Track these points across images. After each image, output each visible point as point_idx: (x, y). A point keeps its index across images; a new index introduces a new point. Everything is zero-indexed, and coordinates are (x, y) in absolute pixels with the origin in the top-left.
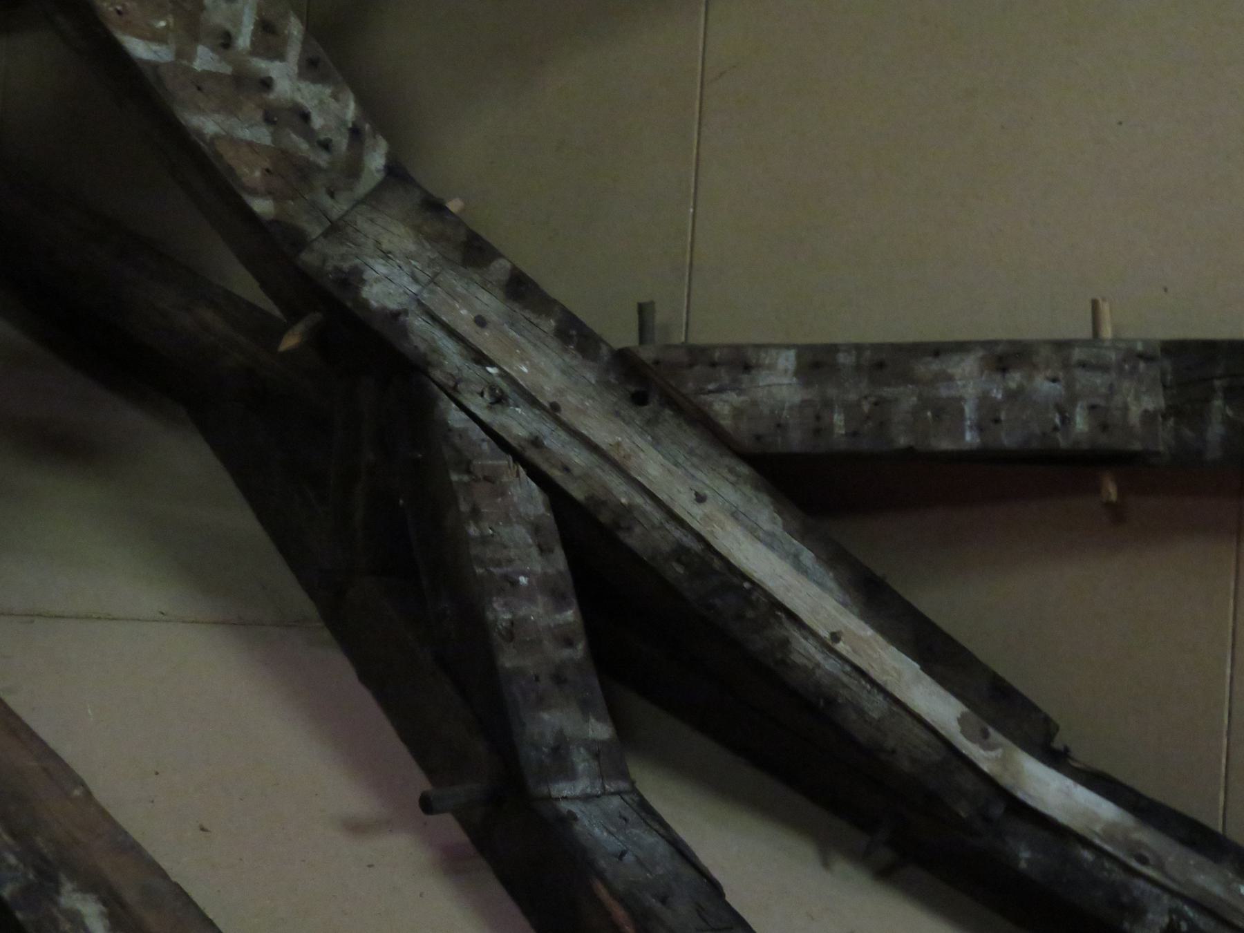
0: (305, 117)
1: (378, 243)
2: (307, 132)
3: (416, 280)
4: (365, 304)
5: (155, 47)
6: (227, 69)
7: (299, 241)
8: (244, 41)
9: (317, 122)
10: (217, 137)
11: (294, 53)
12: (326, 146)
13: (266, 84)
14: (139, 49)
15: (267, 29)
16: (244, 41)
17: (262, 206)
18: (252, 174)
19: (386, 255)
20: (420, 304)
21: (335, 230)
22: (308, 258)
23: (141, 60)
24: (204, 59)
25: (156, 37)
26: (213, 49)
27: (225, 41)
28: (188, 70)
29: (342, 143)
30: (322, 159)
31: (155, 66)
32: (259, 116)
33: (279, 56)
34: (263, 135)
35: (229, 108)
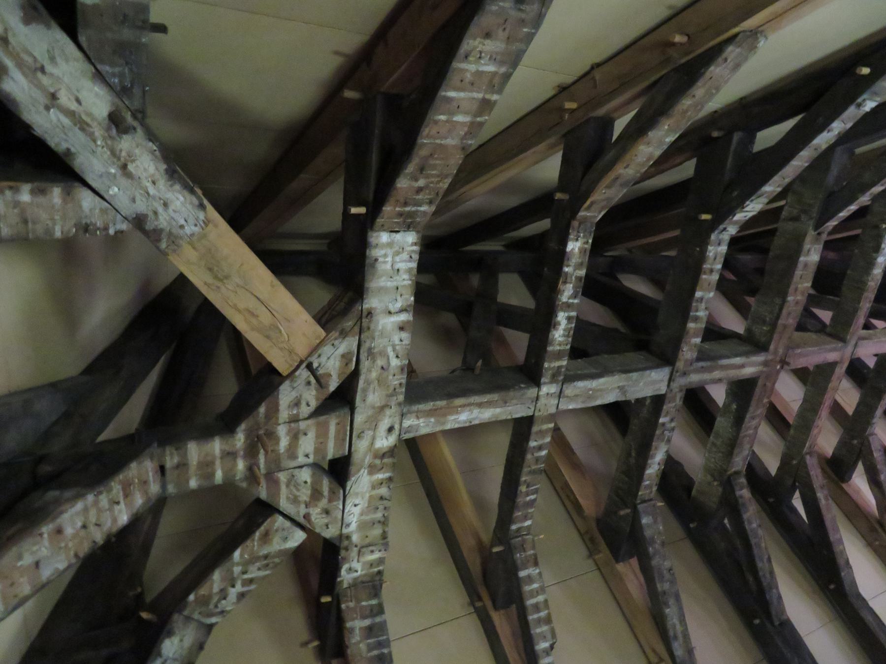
0: (225, 598)
1: (184, 636)
2: (219, 601)
3: (174, 654)
4: (162, 642)
5: (238, 557)
6: (235, 575)
7: (180, 612)
8: (246, 576)
9: (223, 602)
10: (213, 580)
11: (245, 589)
12: (216, 606)
13: (233, 586)
14: (237, 554)
15: (251, 581)
16: (246, 576)
17: (192, 597)
18: (203, 591)
19: (181, 640)
20: (166, 661)
21: (188, 619)
22: (176, 617)
23: (233, 556)
24: (237, 570)
25: (242, 555)
26: (241, 570)
27: (244, 573)
28: (233, 566)
29: (219, 610)
30: (211, 606)
31: (232, 559)
32: (222, 587)
33: (243, 585)
34: (216, 588)
35: (223, 579)
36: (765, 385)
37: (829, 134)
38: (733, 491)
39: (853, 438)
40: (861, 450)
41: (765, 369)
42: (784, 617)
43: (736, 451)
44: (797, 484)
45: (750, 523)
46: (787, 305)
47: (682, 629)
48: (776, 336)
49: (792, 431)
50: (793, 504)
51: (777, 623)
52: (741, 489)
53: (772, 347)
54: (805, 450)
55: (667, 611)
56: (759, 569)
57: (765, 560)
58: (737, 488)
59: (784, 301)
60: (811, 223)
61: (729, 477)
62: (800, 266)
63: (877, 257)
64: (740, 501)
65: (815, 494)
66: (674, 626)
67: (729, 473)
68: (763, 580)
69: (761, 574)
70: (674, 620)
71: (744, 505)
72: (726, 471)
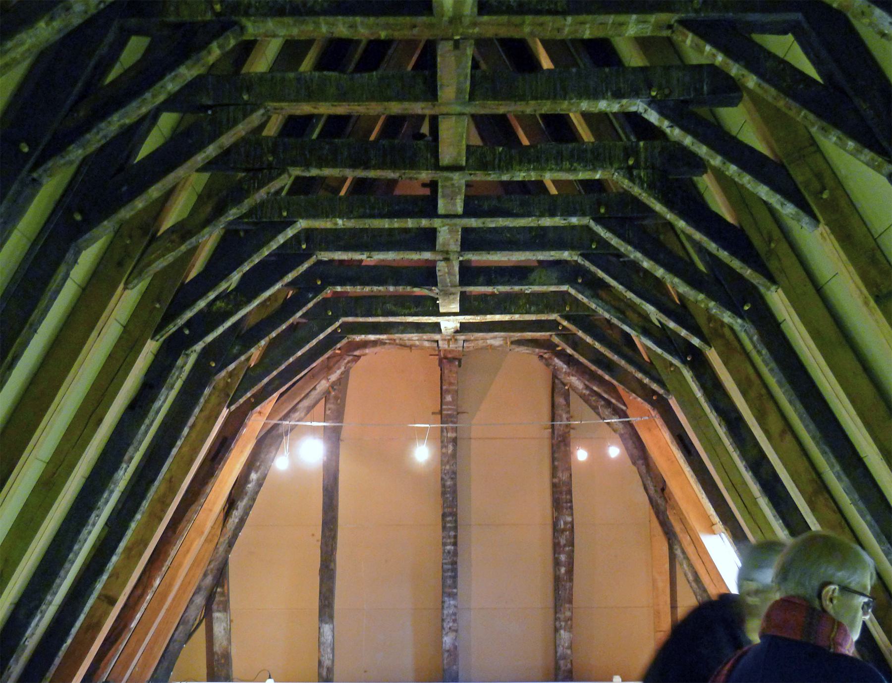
36: (414, 26)
37: (887, 24)
38: (216, 36)
39: (273, 152)
40: (261, 170)
41: (446, 19)
42: (44, 181)
43: (288, 20)
44: (210, 112)
45: (173, 80)
46: (559, 18)
47: (18, 56)
48: (504, 18)
49: (291, 75)
50: (161, 114)
51: (35, 175)
52: (220, 47)
53: (485, 18)
54: (271, 104)
55: (42, 24)
56: (109, 119)
57: (122, 121)
58: (221, 40)
59: (564, 13)
60: (692, 15)
61: (235, 23)
62: (622, 18)
63: (607, 99)
64: (204, 53)
65: (209, 143)
66: (22, 43)
67: (244, 21)
68: (95, 130)
69: (103, 125)
70: (29, 41)
71: (198, 60)
72: (247, 14)
